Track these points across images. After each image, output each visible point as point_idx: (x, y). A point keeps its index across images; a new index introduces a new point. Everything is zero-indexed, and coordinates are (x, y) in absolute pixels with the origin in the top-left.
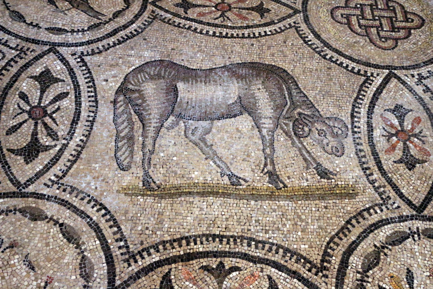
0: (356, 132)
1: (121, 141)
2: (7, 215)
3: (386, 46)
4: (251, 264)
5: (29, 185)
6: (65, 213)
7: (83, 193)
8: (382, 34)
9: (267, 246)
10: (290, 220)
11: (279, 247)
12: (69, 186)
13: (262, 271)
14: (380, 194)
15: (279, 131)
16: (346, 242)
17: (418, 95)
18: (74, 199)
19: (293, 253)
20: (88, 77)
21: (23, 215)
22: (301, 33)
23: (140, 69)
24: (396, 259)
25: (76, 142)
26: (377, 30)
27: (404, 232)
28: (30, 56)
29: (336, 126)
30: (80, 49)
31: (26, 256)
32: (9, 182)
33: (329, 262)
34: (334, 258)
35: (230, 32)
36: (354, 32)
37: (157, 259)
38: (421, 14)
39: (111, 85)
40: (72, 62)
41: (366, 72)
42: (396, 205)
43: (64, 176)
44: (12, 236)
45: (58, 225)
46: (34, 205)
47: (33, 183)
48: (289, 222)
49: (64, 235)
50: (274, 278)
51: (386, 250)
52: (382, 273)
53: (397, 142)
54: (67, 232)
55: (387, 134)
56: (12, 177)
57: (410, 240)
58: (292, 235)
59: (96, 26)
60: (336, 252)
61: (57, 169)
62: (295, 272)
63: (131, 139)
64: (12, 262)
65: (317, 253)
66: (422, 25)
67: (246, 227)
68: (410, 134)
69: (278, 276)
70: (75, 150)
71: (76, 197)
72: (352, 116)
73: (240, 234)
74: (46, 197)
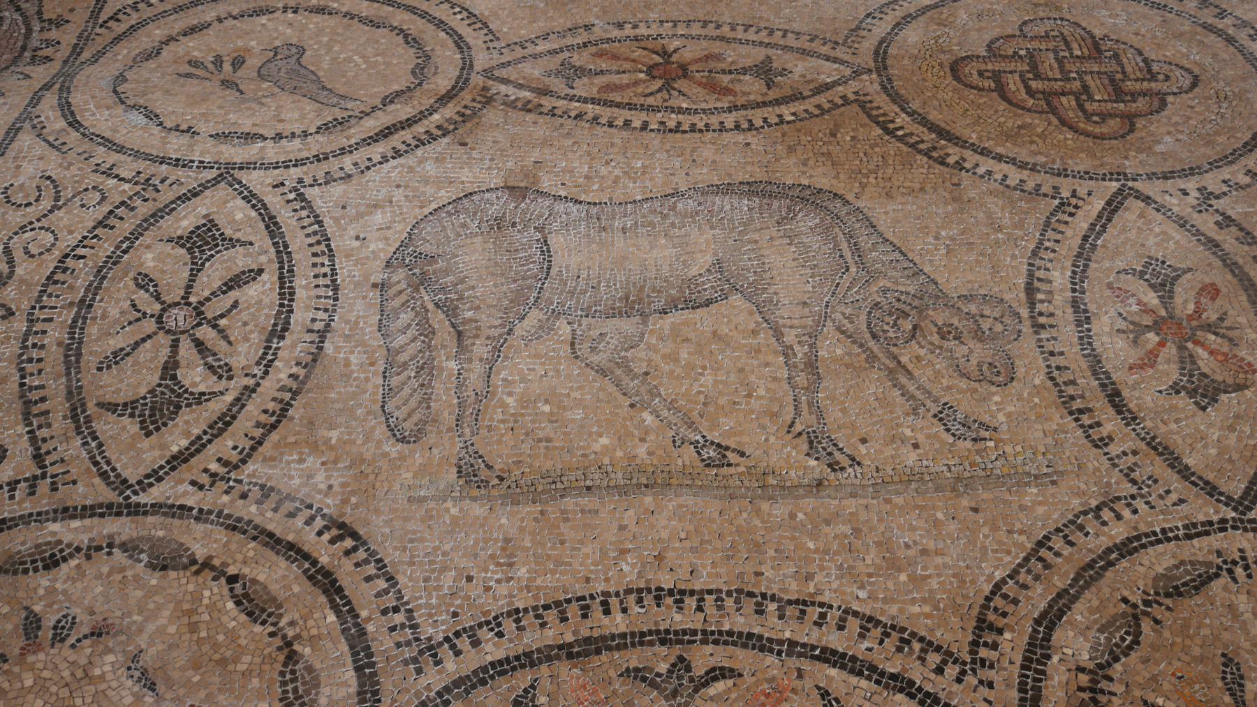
0: (1043, 326)
1: (398, 374)
2: (88, 557)
3: (1105, 130)
5: (151, 485)
6: (245, 549)
7: (294, 500)
12: (255, 485)
14: (1128, 474)
17: (1203, 235)
18: (269, 514)
20: (315, 233)
21: (131, 557)
22: (874, 113)
25: (279, 381)
26: (1077, 99)
28: (167, 195)
29: (987, 312)
30: (295, 172)
31: (135, 658)
32: (97, 481)
34: (1007, 635)
35: (686, 121)
36: (1017, 106)
39: (372, 247)
40: (274, 201)
42: (1174, 497)
43: (244, 462)
44: (99, 608)
45: (223, 580)
46: (161, 533)
47: (160, 479)
49: (238, 603)
51: (1156, 611)
53: (1162, 344)
54: (246, 595)
55: (1132, 327)
56: (105, 467)
57: (1225, 579)
59: (340, 123)
61: (225, 446)
63: (427, 369)
64: (97, 672)
66: (1194, 85)
68: (1194, 323)
70: (274, 399)
71: (275, 510)
72: (1030, 290)
74: (195, 512)
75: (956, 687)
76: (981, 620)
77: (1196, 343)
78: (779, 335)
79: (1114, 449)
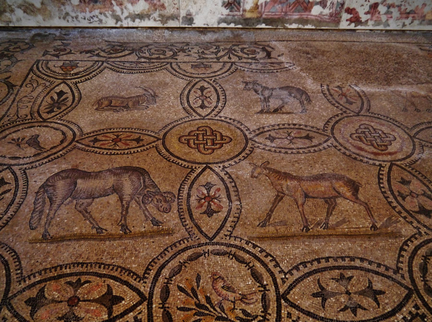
4: (98, 278)
8: (206, 147)
9: (111, 267)
11: (118, 267)
13: (104, 282)
15: (134, 201)
16: (162, 261)
23: (57, 174)
24: (191, 268)
27: (200, 253)
33: (149, 274)
35: (116, 152)
37: (39, 279)
38: (231, 136)
41: (192, 167)
50: (111, 286)
51: (186, 264)
52: (181, 278)
53: (204, 202)
57: (203, 257)
59: (39, 154)
60: (154, 267)
62: (125, 282)
63: (41, 212)
65: (142, 269)
66: (230, 141)
67: (100, 257)
72: (179, 190)
75: (138, 283)
76: (147, 268)
77: (213, 202)
78: (122, 202)
79: (187, 227)
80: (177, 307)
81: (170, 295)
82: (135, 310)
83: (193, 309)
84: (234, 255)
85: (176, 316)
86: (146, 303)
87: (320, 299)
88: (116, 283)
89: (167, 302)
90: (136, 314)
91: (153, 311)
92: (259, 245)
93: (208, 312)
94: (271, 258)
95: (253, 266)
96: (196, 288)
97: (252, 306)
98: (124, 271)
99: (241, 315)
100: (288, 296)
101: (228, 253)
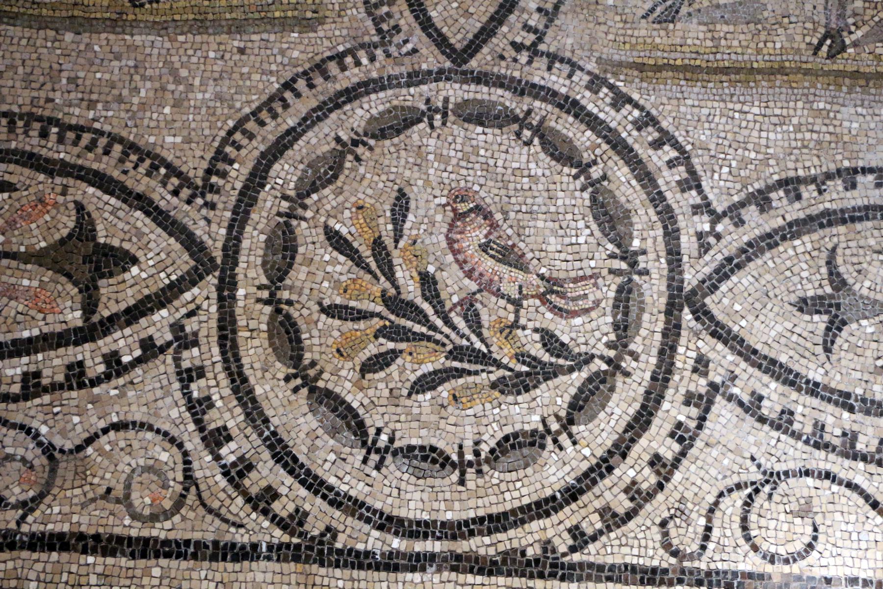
4: (42, 177)
9: (86, 138)
10: (151, 79)
11: (115, 139)
13: (64, 193)
14: (377, 22)
16: (272, 131)
19: (144, 154)
24: (379, 168)
33: (224, 175)
34: (236, 166)
42: (409, 46)
48: (148, 84)
50: (90, 208)
51: (360, 150)
52: (341, 199)
57: (421, 126)
58: (148, 114)
60: (243, 152)
62: (139, 197)
65: (198, 153)
67: (42, 94)
69: (101, 205)
73: (25, 109)
75: (186, 207)
76: (219, 152)
80: (320, 304)
81: (299, 259)
82: (176, 303)
83: (373, 315)
84: (540, 131)
85: (315, 333)
86: (212, 280)
87: (820, 321)
88: (106, 197)
89: (288, 282)
90: (178, 316)
91: (238, 311)
92: (636, 96)
93: (424, 330)
94: (674, 154)
95: (604, 177)
96: (389, 242)
97: (578, 321)
98: (134, 158)
99: (537, 350)
100: (708, 300)
101: (516, 119)
